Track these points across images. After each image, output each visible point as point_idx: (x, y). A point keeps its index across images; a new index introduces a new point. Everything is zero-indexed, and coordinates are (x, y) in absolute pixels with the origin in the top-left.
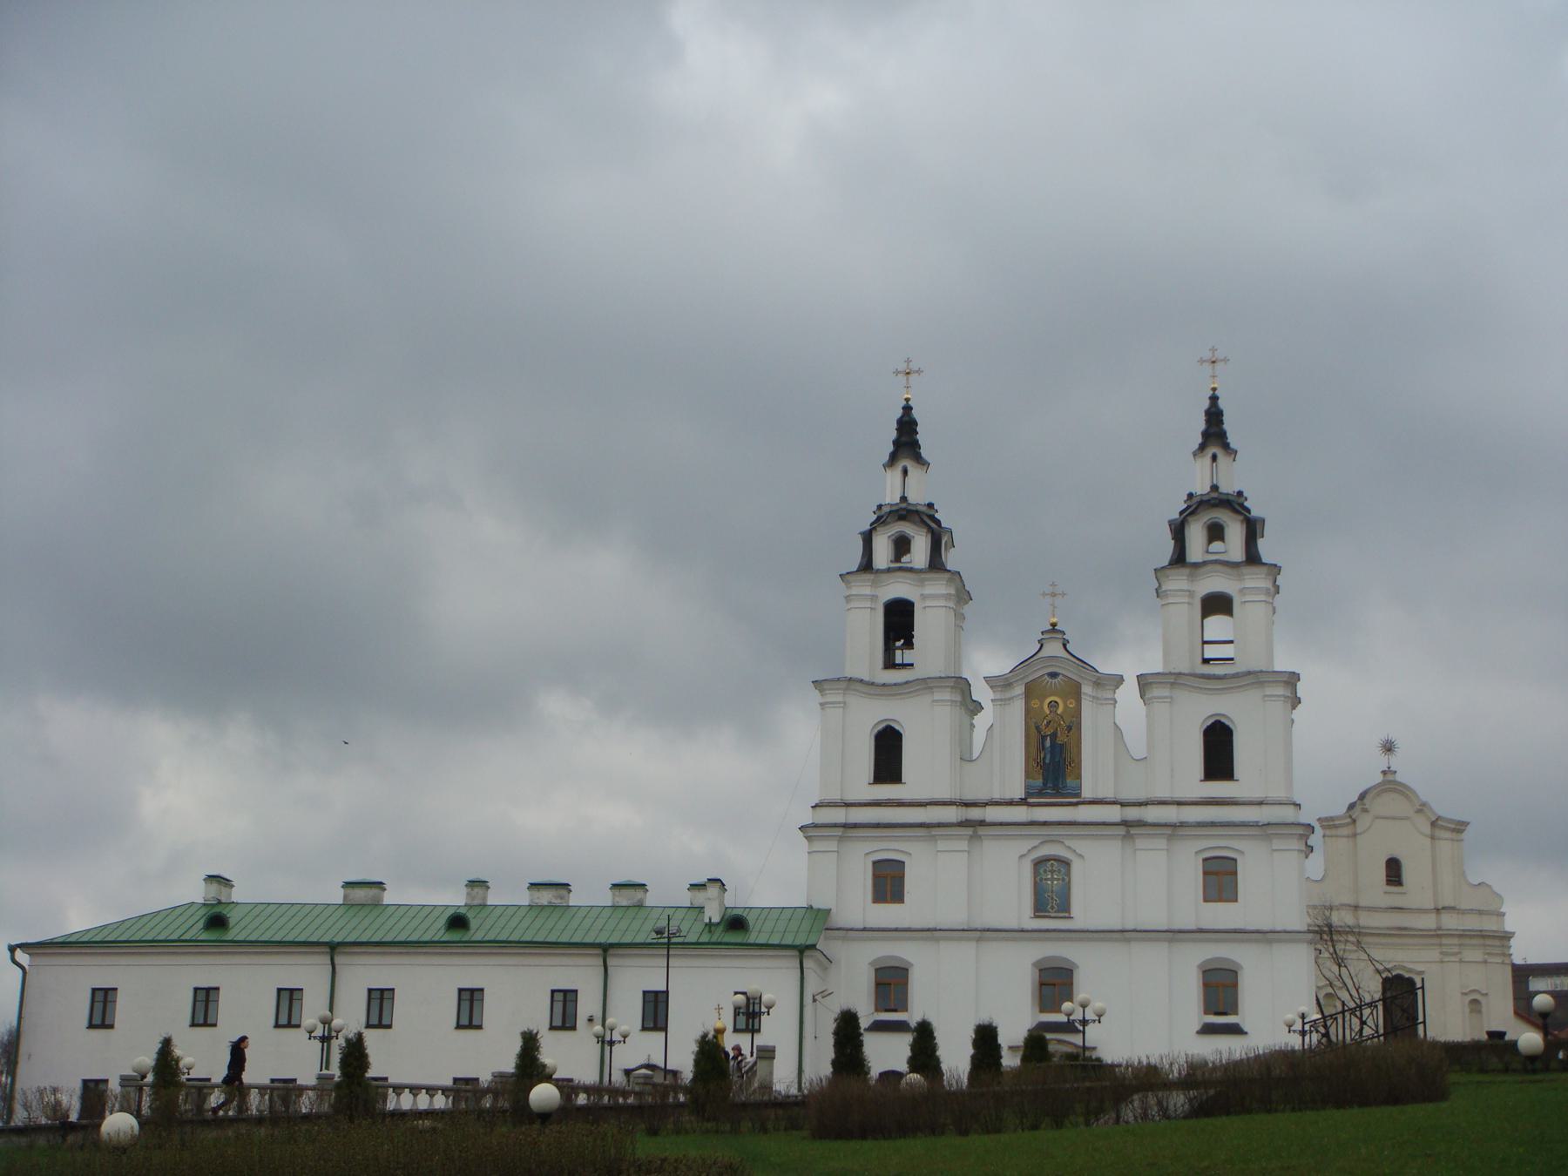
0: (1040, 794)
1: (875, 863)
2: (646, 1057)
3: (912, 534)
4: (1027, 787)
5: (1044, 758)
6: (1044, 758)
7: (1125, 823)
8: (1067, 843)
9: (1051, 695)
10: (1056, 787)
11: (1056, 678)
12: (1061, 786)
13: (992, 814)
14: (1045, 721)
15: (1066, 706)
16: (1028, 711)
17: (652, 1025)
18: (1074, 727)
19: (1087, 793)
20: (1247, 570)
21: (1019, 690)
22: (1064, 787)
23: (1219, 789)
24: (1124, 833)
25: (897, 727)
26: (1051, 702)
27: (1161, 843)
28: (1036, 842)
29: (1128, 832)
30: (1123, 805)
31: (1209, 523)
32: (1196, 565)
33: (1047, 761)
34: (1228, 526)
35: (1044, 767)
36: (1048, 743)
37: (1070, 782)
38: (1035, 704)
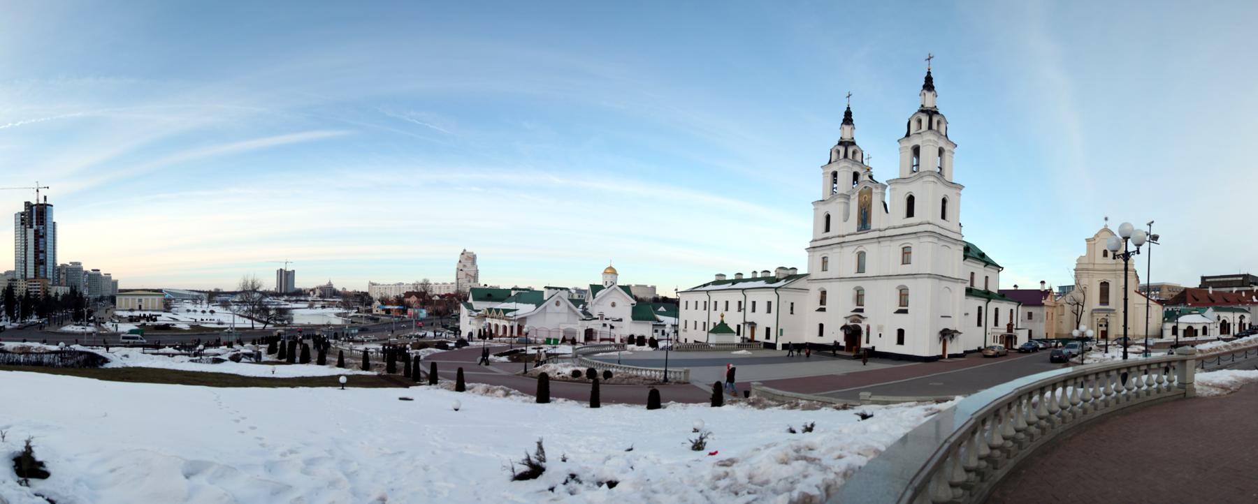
0: (861, 230)
4: (858, 228)
8: (865, 246)
13: (847, 239)
18: (870, 205)
19: (873, 228)
23: (910, 220)
27: (888, 243)
28: (856, 247)
30: (880, 230)
37: (868, 225)
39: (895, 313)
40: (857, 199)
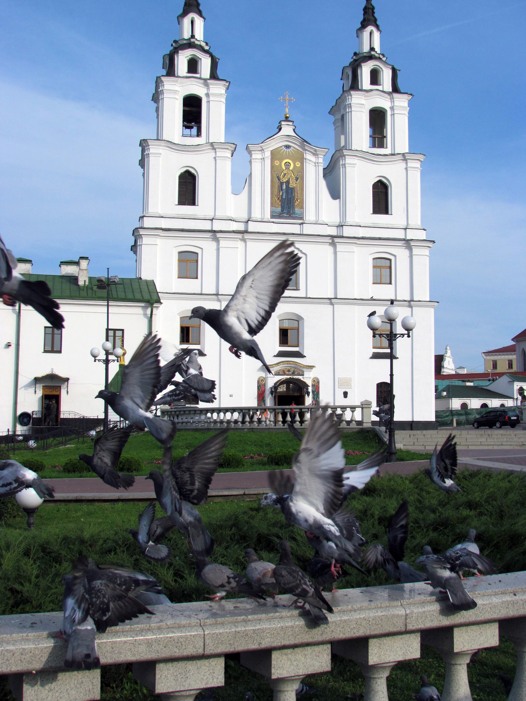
0: (280, 216)
1: (180, 253)
2: (51, 370)
3: (200, 57)
5: (282, 196)
6: (282, 196)
7: (333, 237)
9: (286, 159)
10: (288, 213)
11: (289, 149)
12: (291, 212)
14: (283, 174)
15: (295, 165)
16: (272, 167)
17: (50, 349)
20: (395, 95)
21: (268, 154)
22: (294, 213)
24: (330, 241)
25: (193, 171)
26: (286, 163)
29: (333, 241)
31: (372, 67)
32: (367, 91)
33: (284, 197)
34: (383, 71)
35: (282, 200)
36: (284, 187)
37: (297, 210)
38: (277, 163)
39: (371, 358)
40: (268, 162)
